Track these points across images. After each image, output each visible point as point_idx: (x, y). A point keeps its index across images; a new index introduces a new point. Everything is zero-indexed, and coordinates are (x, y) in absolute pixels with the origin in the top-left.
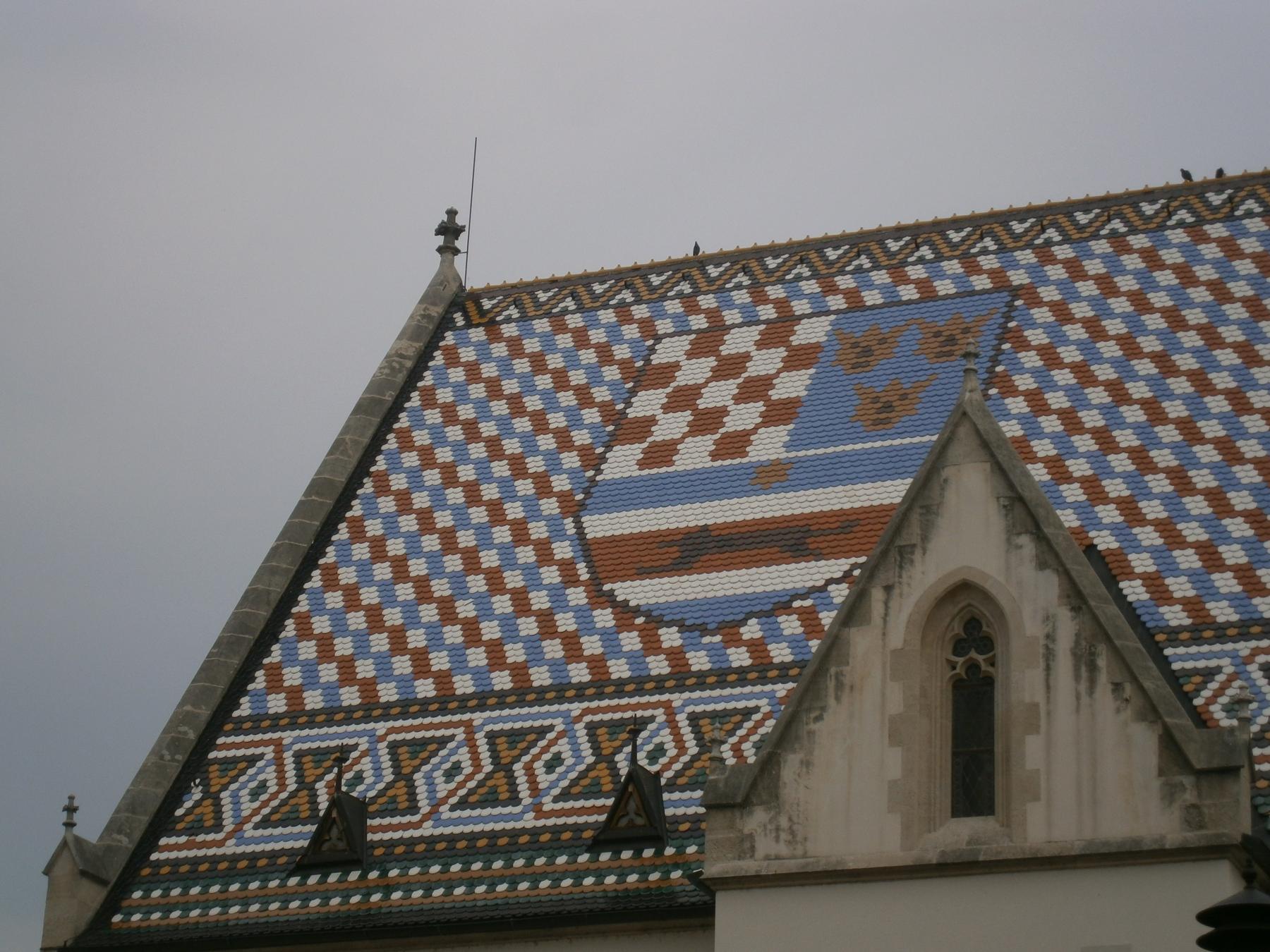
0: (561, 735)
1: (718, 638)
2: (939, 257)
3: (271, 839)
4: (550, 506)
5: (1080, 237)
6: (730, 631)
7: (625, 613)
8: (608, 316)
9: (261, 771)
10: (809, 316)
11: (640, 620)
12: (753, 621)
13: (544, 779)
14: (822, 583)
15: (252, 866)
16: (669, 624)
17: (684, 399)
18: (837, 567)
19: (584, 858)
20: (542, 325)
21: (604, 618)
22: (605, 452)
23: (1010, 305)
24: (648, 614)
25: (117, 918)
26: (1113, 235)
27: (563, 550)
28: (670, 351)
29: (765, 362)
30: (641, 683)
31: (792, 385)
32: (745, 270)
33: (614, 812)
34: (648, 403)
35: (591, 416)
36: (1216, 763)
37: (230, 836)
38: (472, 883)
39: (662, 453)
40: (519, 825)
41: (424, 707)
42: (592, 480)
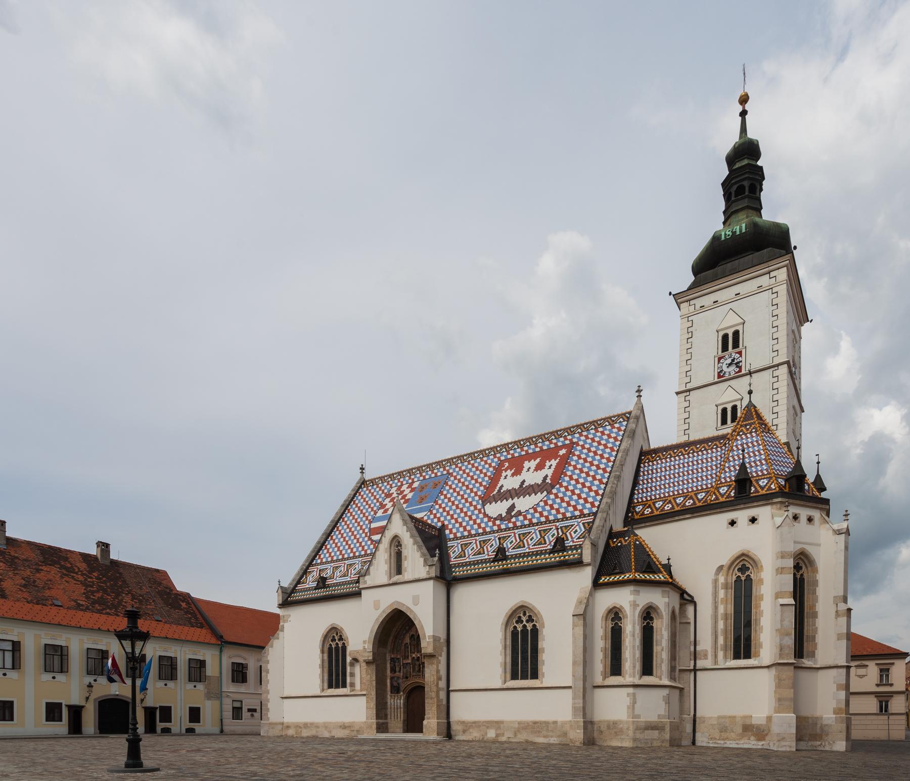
7: (372, 541)
21: (369, 542)
27: (367, 530)
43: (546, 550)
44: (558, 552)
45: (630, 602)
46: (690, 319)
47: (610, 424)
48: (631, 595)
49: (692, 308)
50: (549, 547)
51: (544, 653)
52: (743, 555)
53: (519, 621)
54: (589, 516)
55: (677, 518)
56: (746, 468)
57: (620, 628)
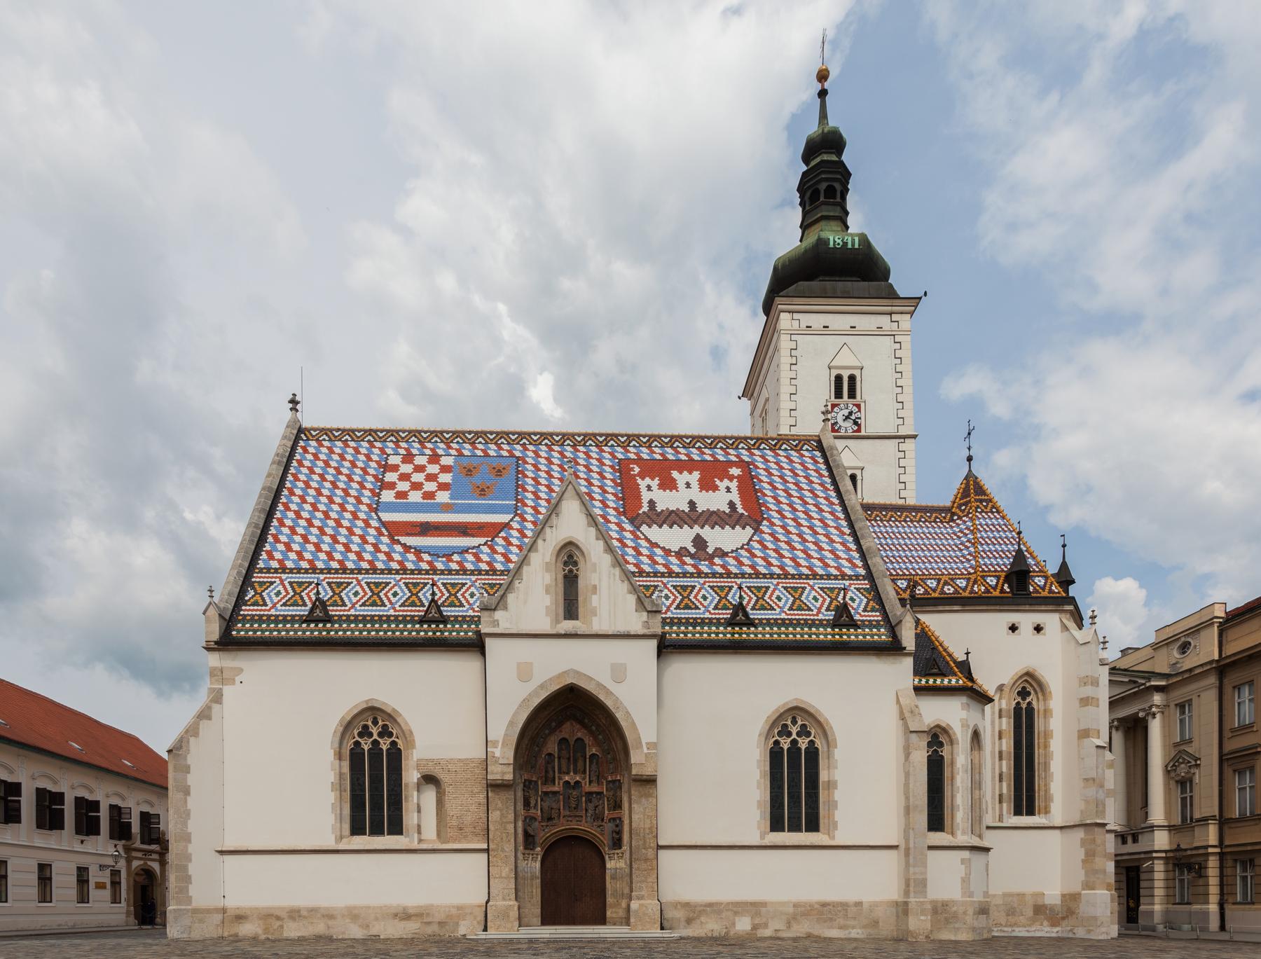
0: (394, 585)
1: (444, 559)
2: (487, 443)
4: (364, 508)
5: (537, 444)
6: (448, 557)
7: (407, 548)
8: (365, 444)
11: (412, 550)
12: (455, 555)
13: (393, 600)
16: (425, 553)
17: (405, 477)
18: (483, 540)
19: (417, 626)
20: (339, 444)
21: (398, 548)
23: (517, 462)
24: (415, 548)
26: (546, 445)
27: (374, 523)
29: (433, 469)
30: (420, 571)
31: (446, 478)
32: (416, 437)
33: (426, 612)
34: (391, 477)
35: (370, 478)
36: (654, 609)
38: (377, 631)
40: (389, 614)
41: (337, 571)
42: (378, 501)
43: (821, 620)
44: (841, 626)
45: (961, 719)
46: (794, 337)
47: (792, 449)
48: (962, 709)
49: (796, 324)
50: (821, 617)
51: (836, 788)
52: (1028, 674)
53: (785, 732)
54: (858, 579)
55: (941, 608)
56: (1025, 558)
57: (940, 758)
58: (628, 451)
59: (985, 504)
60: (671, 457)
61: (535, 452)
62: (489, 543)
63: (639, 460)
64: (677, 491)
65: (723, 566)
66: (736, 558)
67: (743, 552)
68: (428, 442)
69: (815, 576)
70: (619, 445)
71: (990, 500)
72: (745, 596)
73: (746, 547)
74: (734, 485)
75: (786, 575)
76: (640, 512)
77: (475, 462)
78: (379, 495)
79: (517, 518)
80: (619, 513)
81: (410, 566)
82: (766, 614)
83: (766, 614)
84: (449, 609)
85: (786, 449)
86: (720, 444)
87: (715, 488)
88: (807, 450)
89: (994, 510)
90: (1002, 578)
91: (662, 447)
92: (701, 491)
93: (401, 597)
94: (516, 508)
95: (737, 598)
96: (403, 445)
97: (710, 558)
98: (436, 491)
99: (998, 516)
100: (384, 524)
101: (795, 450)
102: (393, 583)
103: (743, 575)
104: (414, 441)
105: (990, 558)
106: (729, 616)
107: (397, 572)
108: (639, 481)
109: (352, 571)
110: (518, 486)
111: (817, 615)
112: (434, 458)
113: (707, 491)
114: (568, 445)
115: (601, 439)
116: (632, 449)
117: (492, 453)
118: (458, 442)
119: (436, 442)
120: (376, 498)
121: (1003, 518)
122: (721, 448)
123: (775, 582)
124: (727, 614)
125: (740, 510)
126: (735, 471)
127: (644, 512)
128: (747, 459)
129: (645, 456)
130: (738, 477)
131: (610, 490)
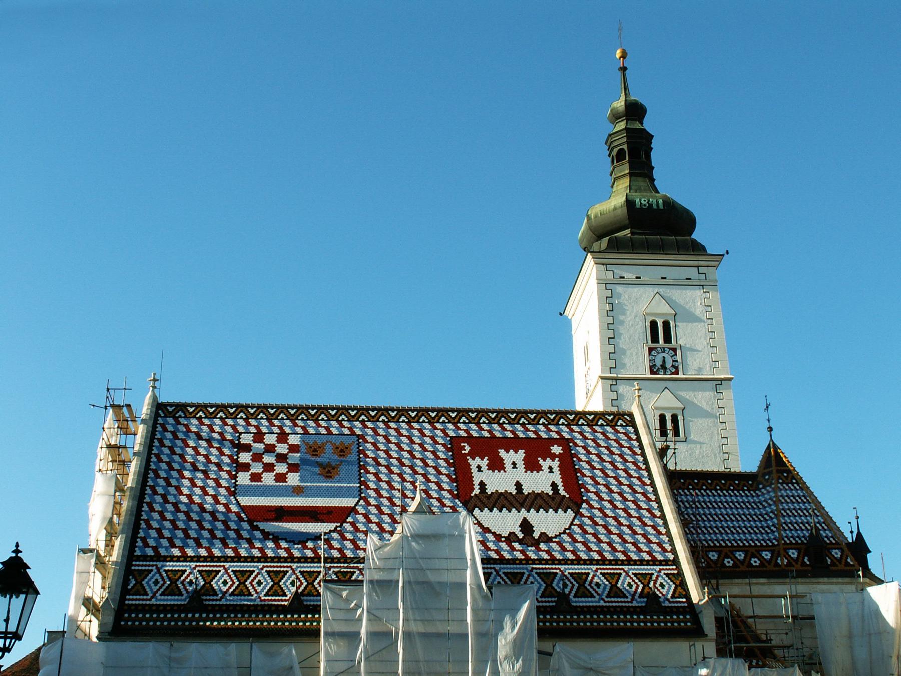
0: (258, 574)
1: (300, 546)
2: (329, 420)
3: (167, 600)
4: (223, 491)
6: (303, 543)
7: (266, 535)
8: (218, 421)
9: (154, 576)
10: (292, 434)
11: (271, 537)
12: (309, 542)
13: (259, 589)
14: (328, 531)
15: (165, 609)
16: (282, 539)
18: (332, 526)
21: (258, 534)
22: (236, 474)
24: (273, 534)
25: (122, 623)
27: (234, 508)
28: (246, 439)
29: (282, 449)
30: (279, 559)
31: (295, 457)
32: (264, 413)
34: (245, 457)
37: (152, 597)
39: (256, 477)
41: (205, 559)
42: (235, 483)
50: (634, 604)
58: (458, 428)
59: (785, 475)
60: (498, 434)
61: (374, 429)
62: (339, 529)
63: (469, 439)
64: (505, 472)
65: (548, 552)
66: (559, 543)
67: (565, 537)
68: (275, 419)
69: (629, 561)
70: (449, 422)
71: (789, 472)
72: (568, 583)
73: (567, 531)
74: (556, 464)
75: (603, 561)
76: (472, 495)
77: (320, 440)
78: (235, 477)
79: (362, 502)
80: (455, 497)
81: (270, 554)
82: (586, 602)
83: (586, 602)
84: (309, 598)
85: (602, 425)
86: (542, 420)
87: (539, 468)
88: (621, 425)
89: (794, 481)
90: (803, 551)
91: (490, 423)
92: (526, 472)
93: (266, 586)
94: (360, 491)
95: (561, 585)
96: (253, 422)
97: (536, 543)
98: (287, 473)
99: (798, 488)
100: (244, 508)
101: (613, 427)
102: (257, 572)
103: (566, 562)
104: (262, 418)
105: (791, 530)
106: (554, 604)
107: (259, 560)
108: (470, 461)
109: (219, 559)
110: (361, 467)
111: (631, 602)
112: (283, 437)
113: (532, 472)
114: (403, 421)
115: (433, 415)
116: (461, 426)
117: (335, 431)
118: (302, 419)
119: (282, 419)
120: (233, 481)
121: (802, 489)
122: (543, 424)
123: (594, 568)
124: (552, 602)
125: (562, 492)
126: (556, 449)
127: (475, 494)
128: (567, 436)
129: (475, 434)
130: (560, 455)
131: (444, 471)
